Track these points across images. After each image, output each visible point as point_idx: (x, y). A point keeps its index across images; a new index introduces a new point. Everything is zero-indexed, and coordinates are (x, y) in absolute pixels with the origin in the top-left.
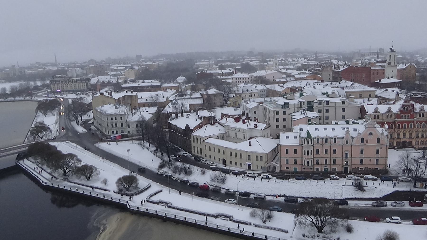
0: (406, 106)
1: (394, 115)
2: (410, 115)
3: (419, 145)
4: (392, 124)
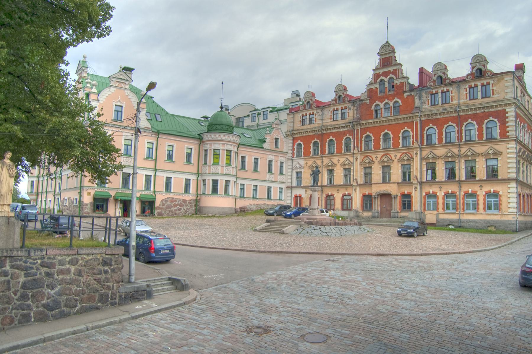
0: (386, 74)
1: (352, 108)
2: (400, 101)
3: (440, 210)
4: (348, 136)
